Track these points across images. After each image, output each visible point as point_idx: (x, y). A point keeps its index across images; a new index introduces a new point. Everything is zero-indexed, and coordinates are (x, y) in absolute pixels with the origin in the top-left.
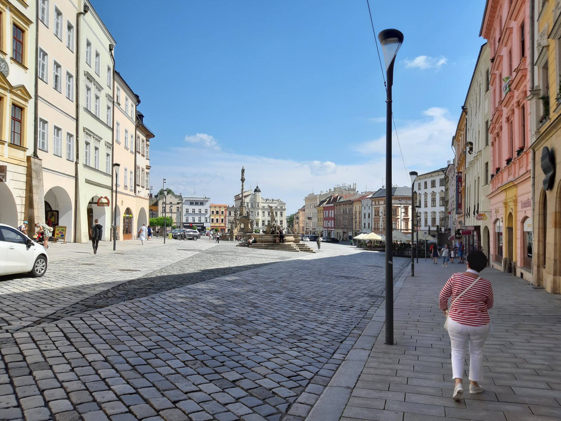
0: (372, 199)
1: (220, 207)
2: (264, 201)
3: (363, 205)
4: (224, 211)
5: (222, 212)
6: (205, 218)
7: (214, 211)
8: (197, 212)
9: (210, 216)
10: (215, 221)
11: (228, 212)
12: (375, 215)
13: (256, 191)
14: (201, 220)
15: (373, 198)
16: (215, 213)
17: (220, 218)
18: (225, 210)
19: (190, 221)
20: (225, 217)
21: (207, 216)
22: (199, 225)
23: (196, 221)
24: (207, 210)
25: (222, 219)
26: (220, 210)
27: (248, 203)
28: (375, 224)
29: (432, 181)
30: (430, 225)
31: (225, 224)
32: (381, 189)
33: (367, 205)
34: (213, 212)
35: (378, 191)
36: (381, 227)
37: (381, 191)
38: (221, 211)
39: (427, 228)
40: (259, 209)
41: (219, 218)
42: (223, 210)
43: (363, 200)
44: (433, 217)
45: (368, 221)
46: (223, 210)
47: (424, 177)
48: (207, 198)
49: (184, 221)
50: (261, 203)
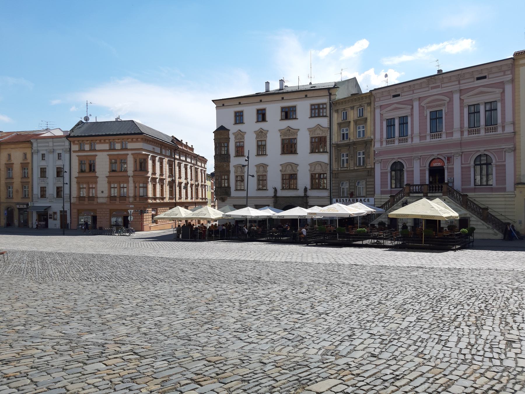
0: (70, 139)
3: (38, 151)
12: (82, 171)
15: (74, 137)
28: (79, 189)
29: (283, 109)
30: (279, 186)
32: (81, 122)
33: (53, 151)
35: (78, 125)
36: (99, 195)
37: (85, 126)
39: (270, 193)
43: (39, 140)
44: (289, 171)
45: (38, 184)
47: (258, 99)
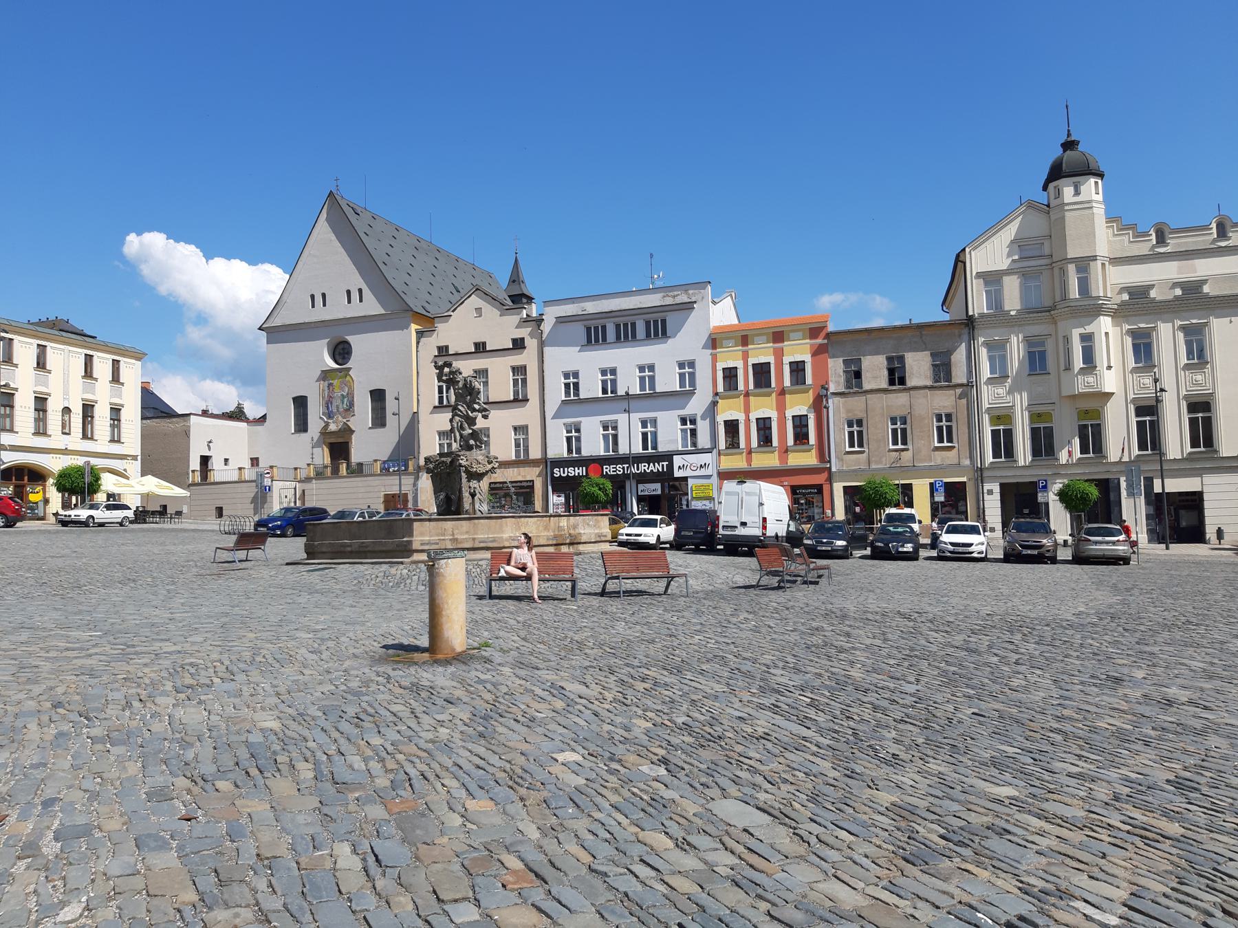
1: (778, 337)
2: (1143, 248)
4: (807, 358)
5: (798, 369)
6: (683, 421)
7: (739, 364)
8: (629, 383)
9: (715, 403)
10: (749, 436)
11: (836, 367)
13: (1056, 173)
14: (659, 439)
16: (745, 380)
17: (781, 408)
18: (817, 352)
19: (593, 445)
20: (819, 404)
21: (696, 406)
22: (644, 467)
23: (623, 449)
24: (692, 364)
25: (800, 424)
26: (779, 354)
27: (992, 279)
31: (823, 455)
34: (730, 374)
38: (787, 359)
40: (1093, 310)
41: (773, 414)
42: (799, 350)
46: (799, 350)
48: (685, 287)
49: (558, 449)
50: (1116, 261)
